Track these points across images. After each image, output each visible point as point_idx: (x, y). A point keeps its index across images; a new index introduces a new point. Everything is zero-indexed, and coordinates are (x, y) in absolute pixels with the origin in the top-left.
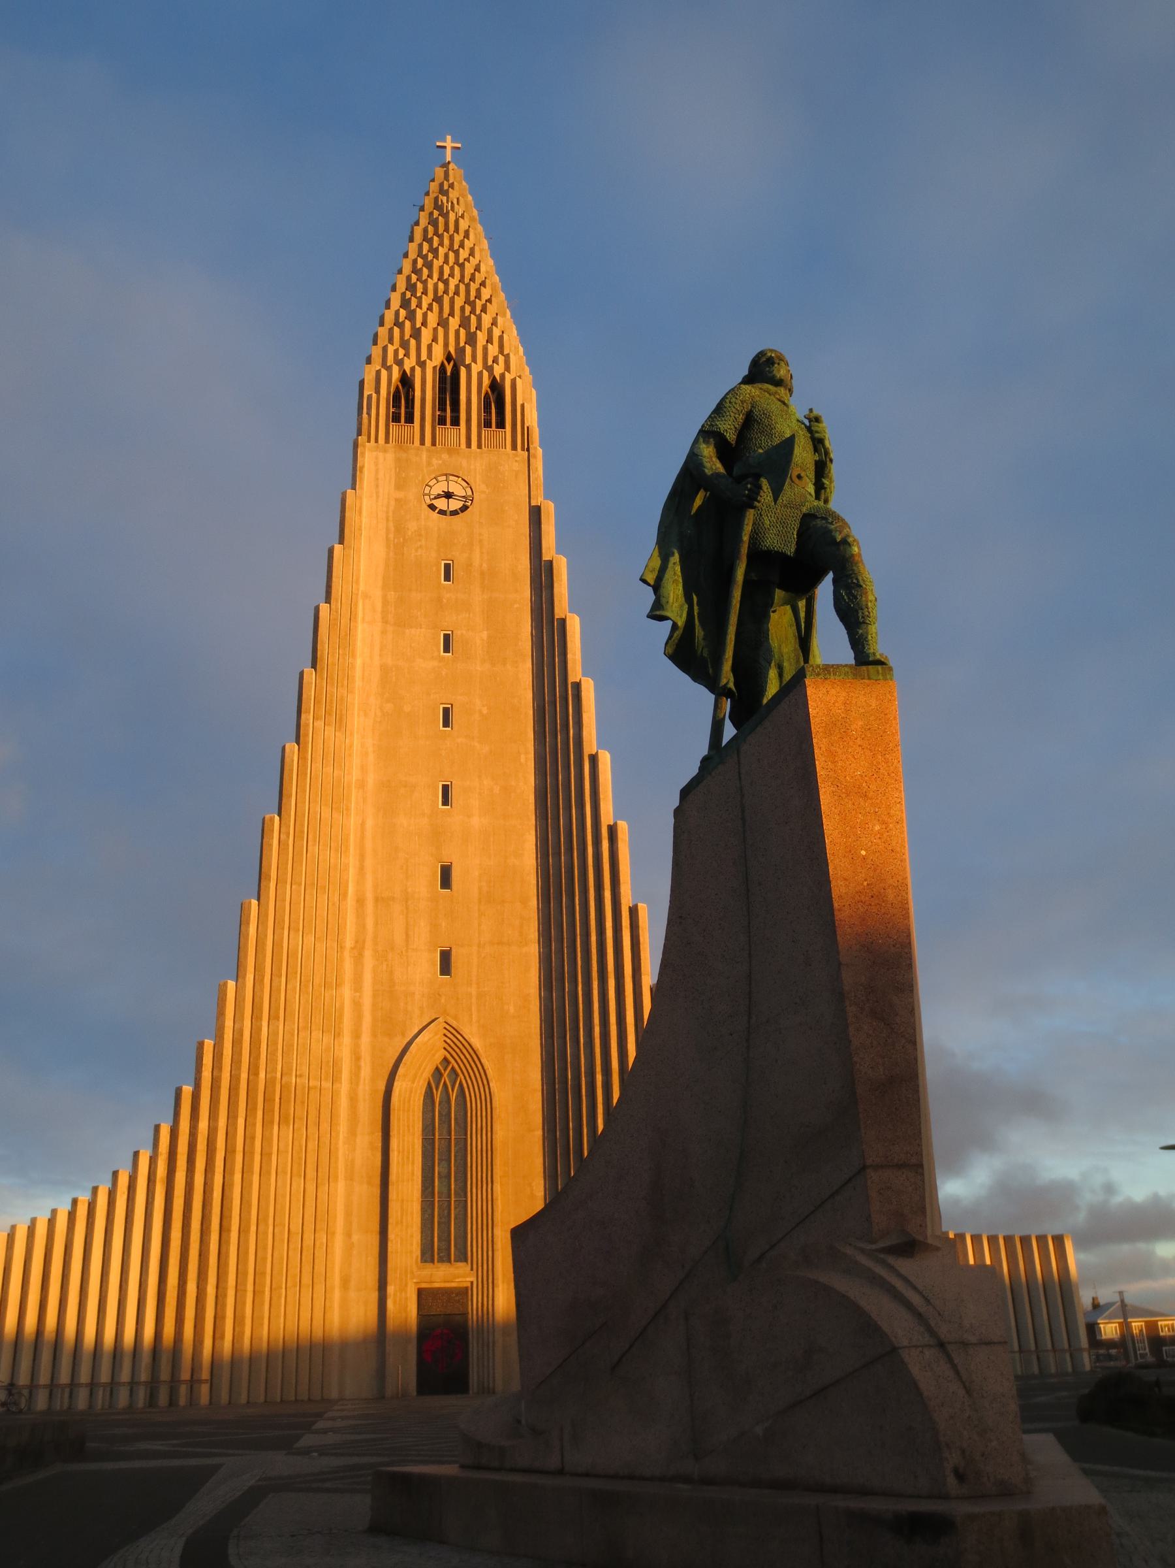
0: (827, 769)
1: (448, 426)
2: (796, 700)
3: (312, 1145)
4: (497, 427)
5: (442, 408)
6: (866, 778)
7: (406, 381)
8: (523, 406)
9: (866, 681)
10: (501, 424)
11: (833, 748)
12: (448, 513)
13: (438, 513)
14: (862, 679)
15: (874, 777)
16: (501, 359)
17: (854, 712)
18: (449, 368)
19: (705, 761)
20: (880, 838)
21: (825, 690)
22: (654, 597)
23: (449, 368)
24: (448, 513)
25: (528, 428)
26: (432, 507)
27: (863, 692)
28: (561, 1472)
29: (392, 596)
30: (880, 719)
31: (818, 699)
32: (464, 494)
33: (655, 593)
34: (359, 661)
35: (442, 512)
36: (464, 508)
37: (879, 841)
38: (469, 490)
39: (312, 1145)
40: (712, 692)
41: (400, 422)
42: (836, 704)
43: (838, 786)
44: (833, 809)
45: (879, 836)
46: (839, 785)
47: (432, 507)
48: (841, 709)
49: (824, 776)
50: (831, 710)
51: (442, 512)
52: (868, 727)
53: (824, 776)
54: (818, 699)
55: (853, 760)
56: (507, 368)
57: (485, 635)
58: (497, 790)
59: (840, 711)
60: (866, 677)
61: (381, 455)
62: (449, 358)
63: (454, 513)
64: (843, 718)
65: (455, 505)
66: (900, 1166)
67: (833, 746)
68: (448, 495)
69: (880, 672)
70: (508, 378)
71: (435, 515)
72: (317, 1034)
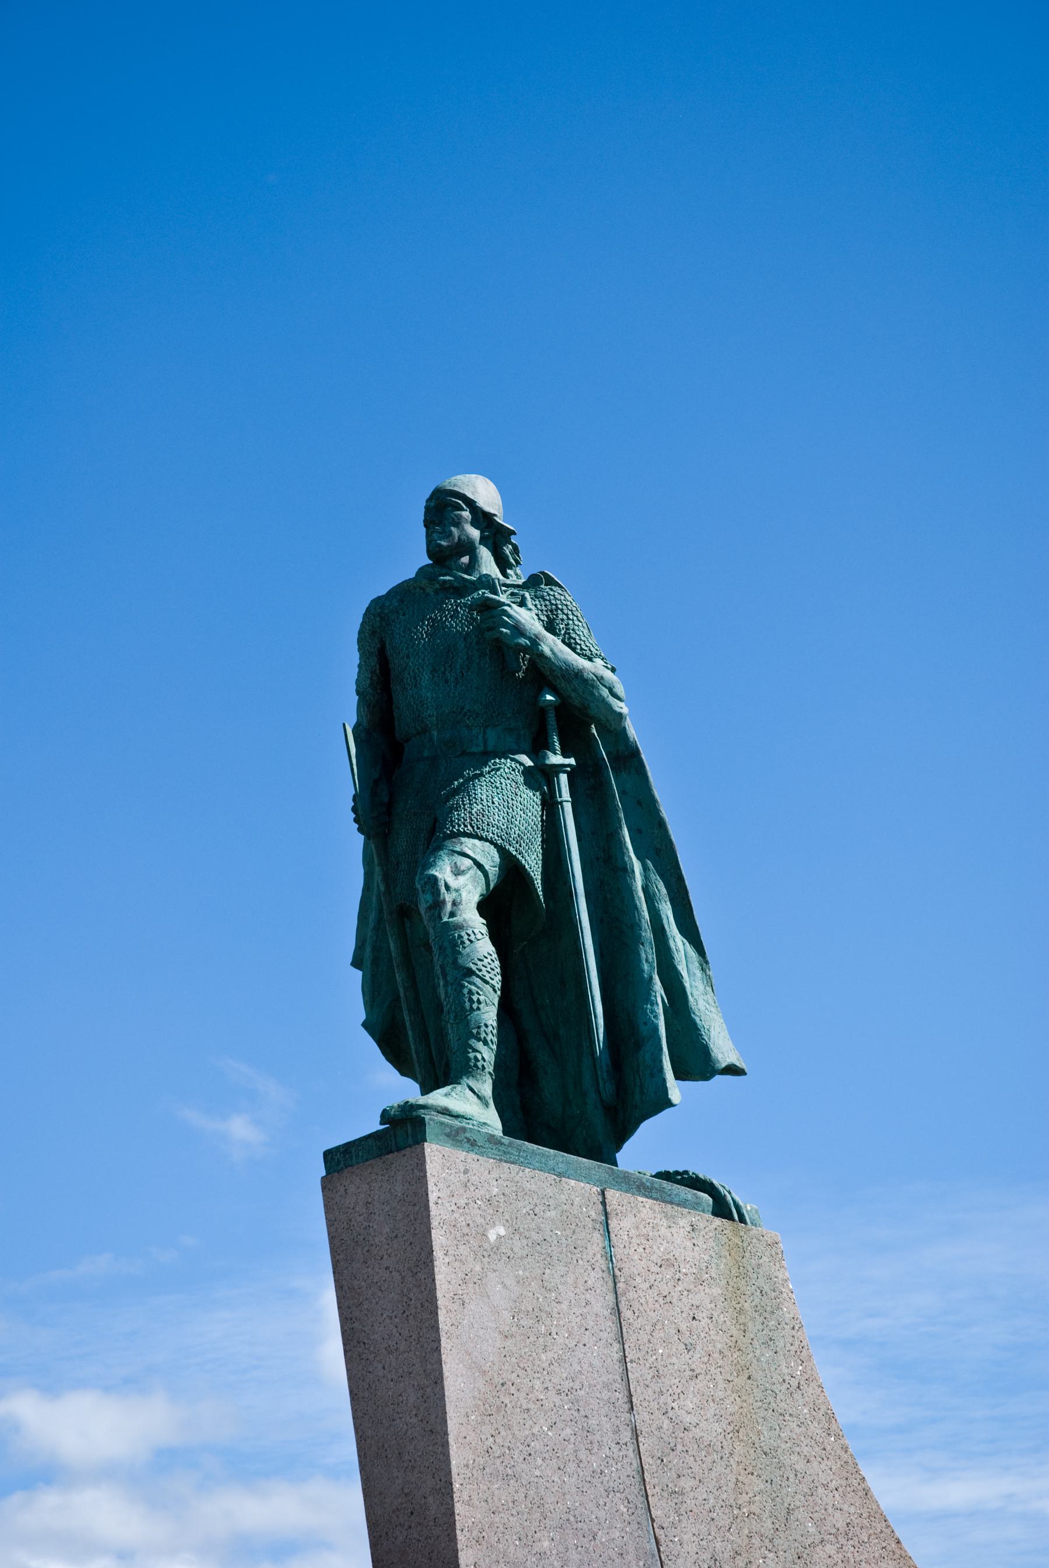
6: (397, 1320)
15: (405, 1315)
17: (377, 1214)
20: (416, 1415)
21: (342, 1189)
30: (408, 1215)
37: (414, 1420)
43: (364, 1343)
44: (361, 1381)
45: (414, 1413)
46: (366, 1341)
50: (351, 1221)
54: (335, 1208)
55: (380, 1294)
67: (356, 1278)
69: (410, 1131)
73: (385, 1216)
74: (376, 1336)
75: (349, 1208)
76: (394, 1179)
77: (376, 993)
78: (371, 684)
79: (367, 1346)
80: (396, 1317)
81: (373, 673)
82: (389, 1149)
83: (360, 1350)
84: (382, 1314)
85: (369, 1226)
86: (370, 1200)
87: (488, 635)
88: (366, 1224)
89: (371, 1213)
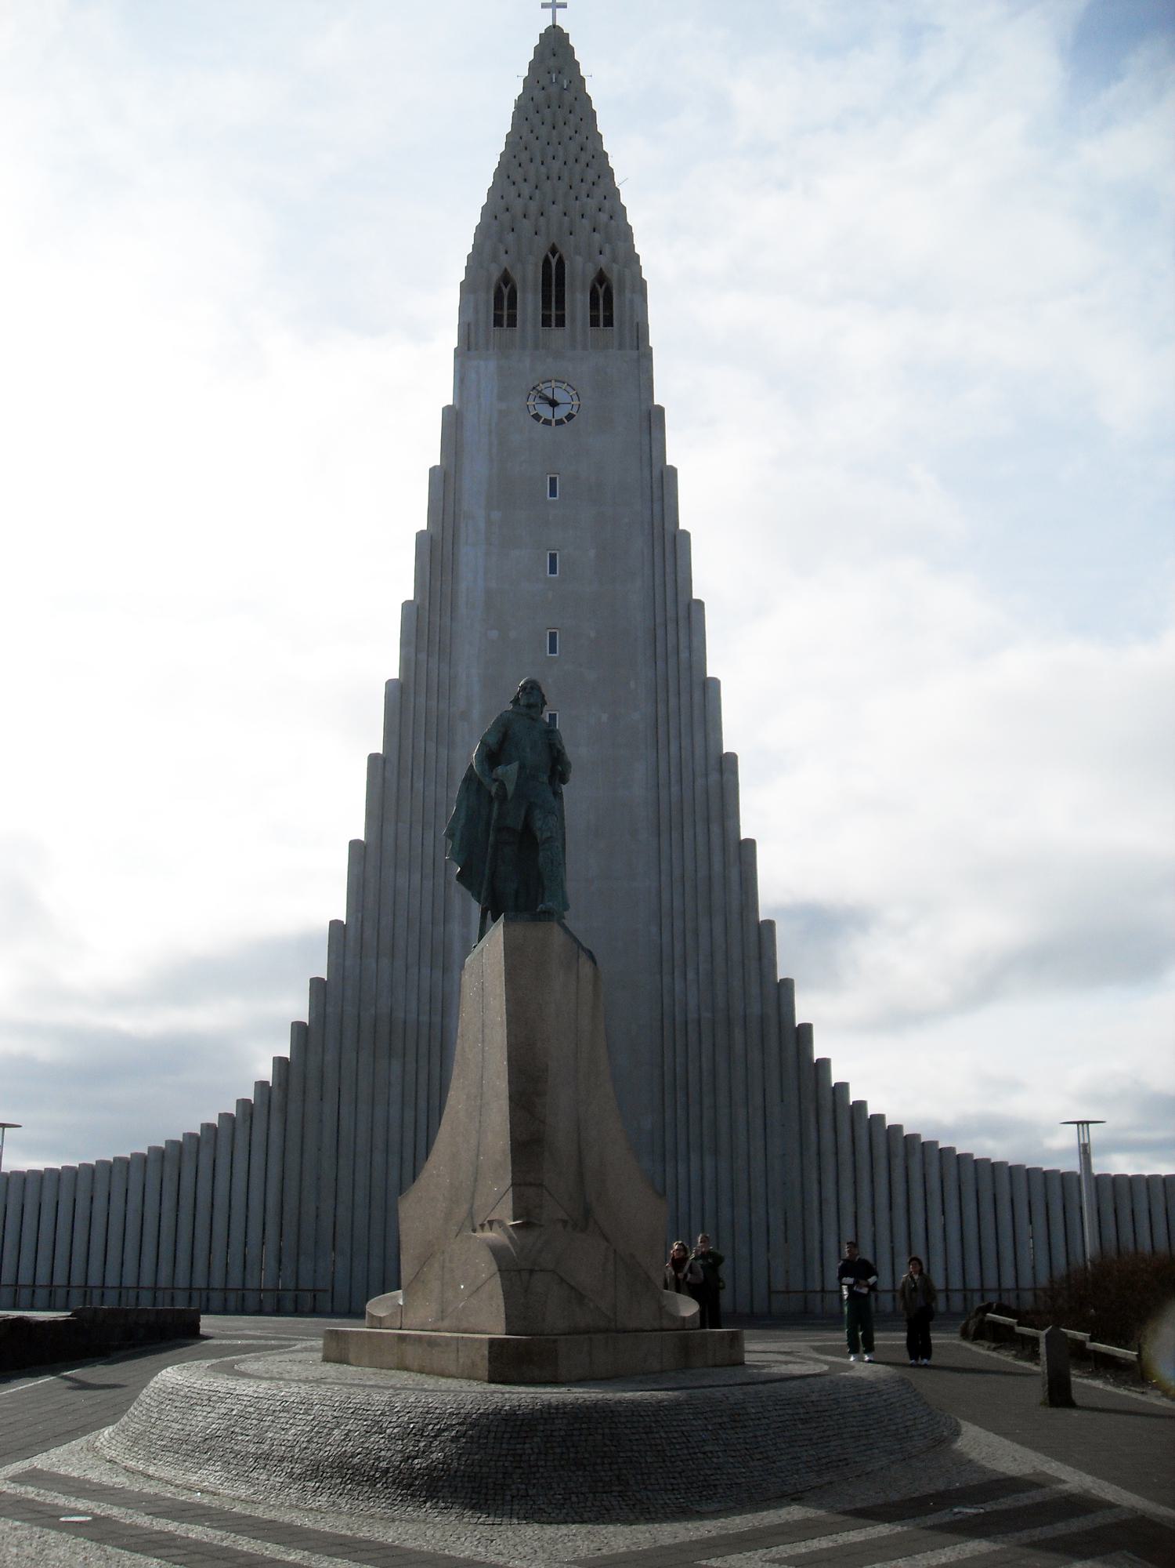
1: (553, 327)
3: (423, 1077)
4: (605, 326)
5: (546, 304)
7: (506, 279)
8: (632, 302)
10: (609, 322)
12: (554, 423)
13: (543, 423)
16: (607, 249)
18: (554, 262)
23: (554, 262)
24: (554, 423)
25: (638, 324)
26: (537, 417)
28: (400, 1329)
29: (496, 515)
32: (570, 401)
34: (463, 586)
35: (547, 422)
36: (570, 417)
38: (575, 397)
39: (423, 1077)
41: (502, 326)
47: (537, 417)
51: (547, 422)
56: (614, 260)
57: (592, 553)
58: (605, 717)
61: (482, 363)
62: (554, 250)
63: (560, 422)
65: (561, 413)
66: (531, 1184)
68: (553, 404)
70: (615, 267)
71: (539, 425)
72: (426, 971)
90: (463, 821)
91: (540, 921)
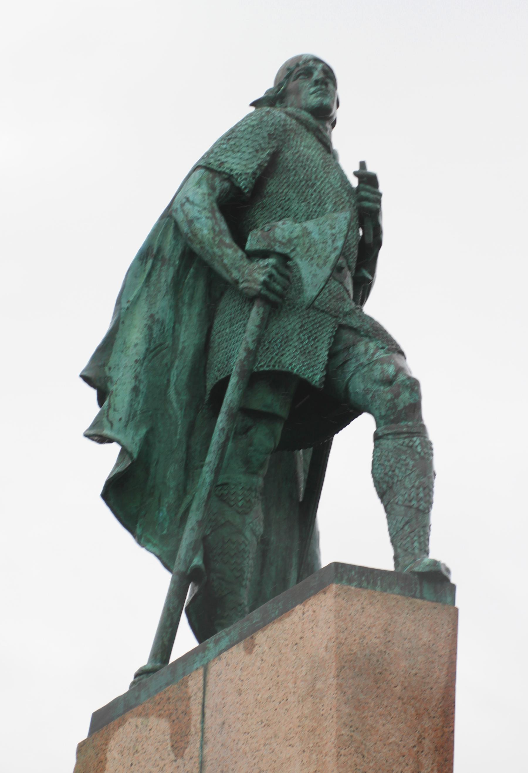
0: (351, 727)
2: (314, 611)
9: (419, 601)
11: (362, 697)
14: (414, 596)
19: (141, 674)
21: (358, 606)
22: (96, 410)
27: (412, 617)
30: (433, 662)
31: (348, 619)
33: (101, 400)
40: (168, 567)
42: (374, 630)
46: (366, 755)
48: (379, 638)
49: (346, 737)
50: (364, 638)
52: (414, 672)
53: (346, 737)
54: (348, 619)
59: (377, 641)
60: (418, 594)
64: (380, 651)
73: (406, 651)
74: (378, 756)
75: (364, 625)
76: (421, 623)
77: (131, 417)
78: (254, 173)
79: (365, 759)
80: (404, 747)
81: (260, 166)
82: (413, 593)
83: (358, 761)
84: (388, 738)
85: (385, 652)
86: (390, 628)
87: (367, 204)
88: (382, 648)
89: (389, 641)
90: (142, 348)
91: (422, 598)
